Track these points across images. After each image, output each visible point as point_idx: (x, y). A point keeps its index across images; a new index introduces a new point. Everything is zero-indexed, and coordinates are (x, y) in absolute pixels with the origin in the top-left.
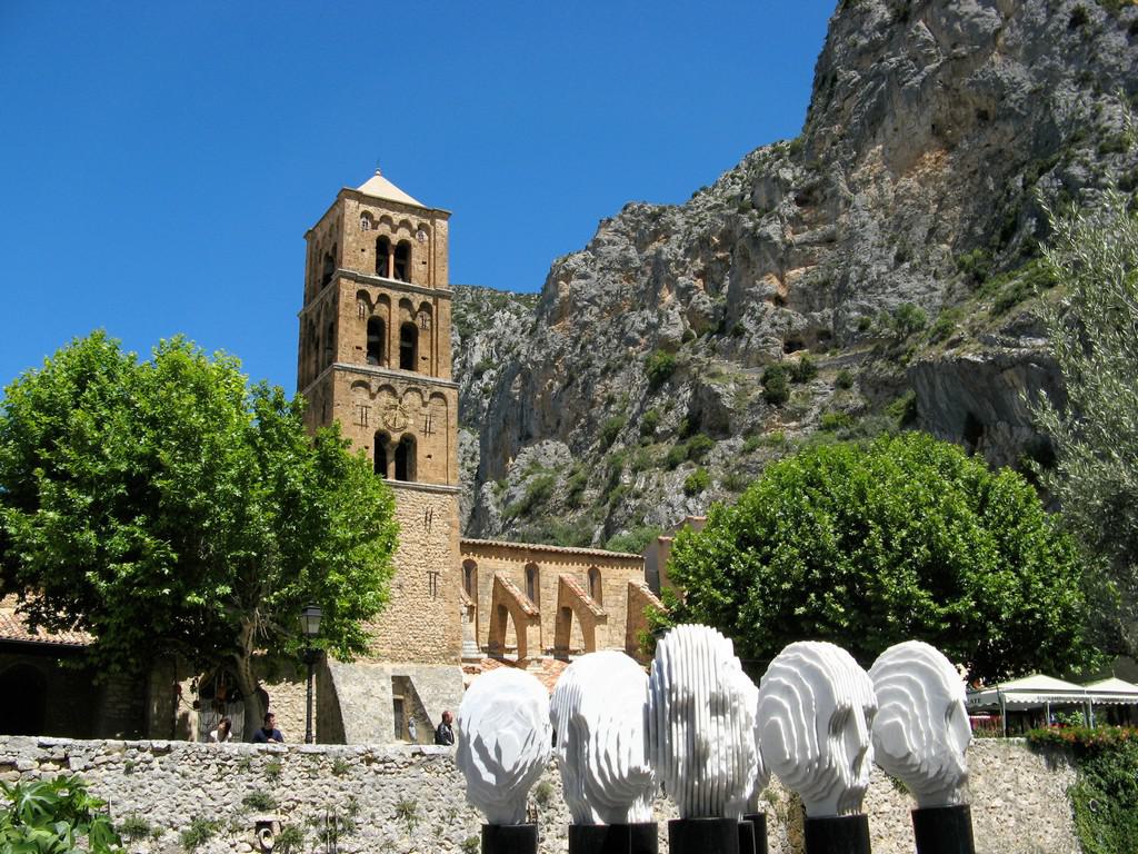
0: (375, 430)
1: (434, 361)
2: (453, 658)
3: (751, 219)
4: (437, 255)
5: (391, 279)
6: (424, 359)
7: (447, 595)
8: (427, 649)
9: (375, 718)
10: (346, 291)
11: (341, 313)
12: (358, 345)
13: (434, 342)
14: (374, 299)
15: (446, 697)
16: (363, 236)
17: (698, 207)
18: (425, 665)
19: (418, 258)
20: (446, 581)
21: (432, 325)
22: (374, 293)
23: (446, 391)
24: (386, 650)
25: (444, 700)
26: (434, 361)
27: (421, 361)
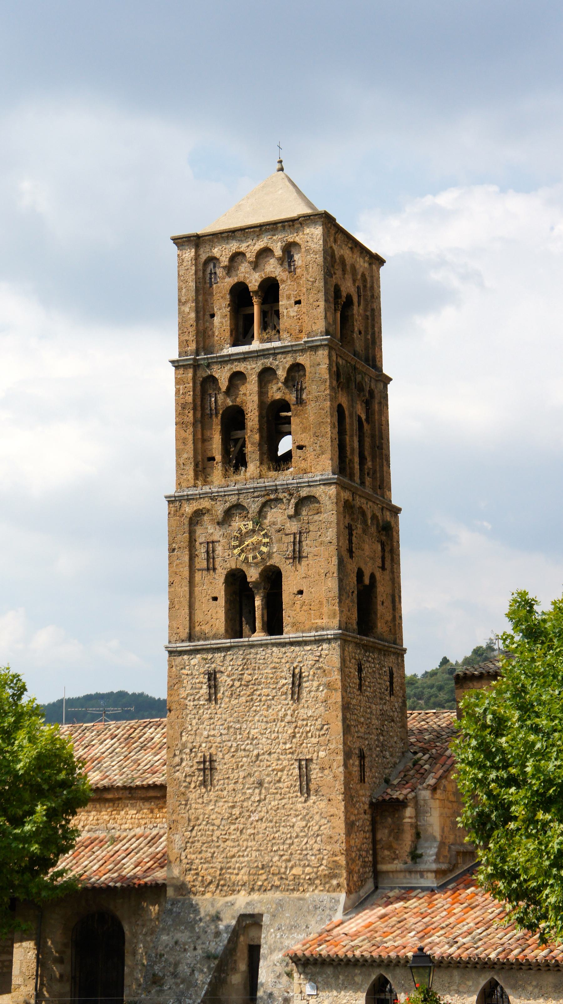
0: (225, 572)
2: (335, 882)
7: (324, 791)
18: (296, 895)
19: (289, 298)
20: (322, 769)
23: (318, 491)
24: (243, 876)
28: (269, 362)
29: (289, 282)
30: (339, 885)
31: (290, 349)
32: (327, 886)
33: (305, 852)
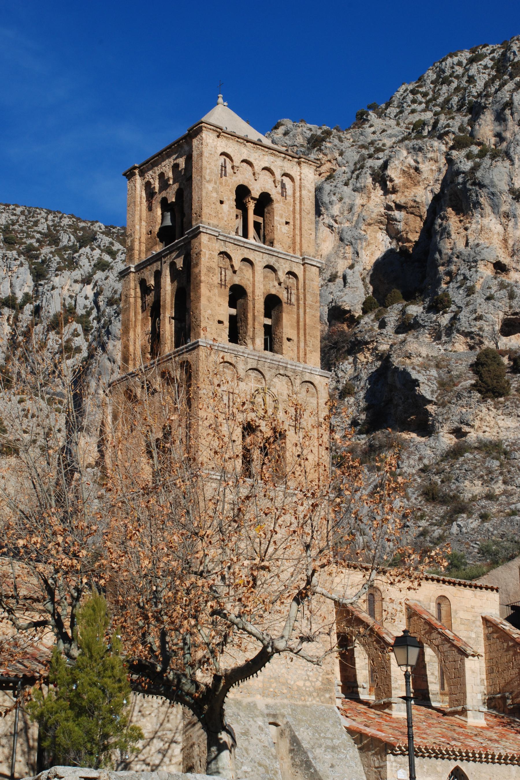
1: (302, 344)
2: (327, 696)
3: (469, 157)
4: (303, 214)
5: (252, 241)
6: (289, 340)
8: (301, 683)
9: (260, 765)
10: (207, 253)
11: (203, 278)
12: (221, 319)
13: (301, 319)
14: (237, 263)
15: (329, 742)
16: (221, 183)
17: (374, 133)
19: (281, 217)
21: (298, 300)
22: (237, 256)
25: (327, 747)
26: (302, 344)
27: (286, 343)
28: (272, 261)
29: (281, 204)
30: (330, 698)
31: (289, 258)
32: (322, 698)
33: (306, 669)
